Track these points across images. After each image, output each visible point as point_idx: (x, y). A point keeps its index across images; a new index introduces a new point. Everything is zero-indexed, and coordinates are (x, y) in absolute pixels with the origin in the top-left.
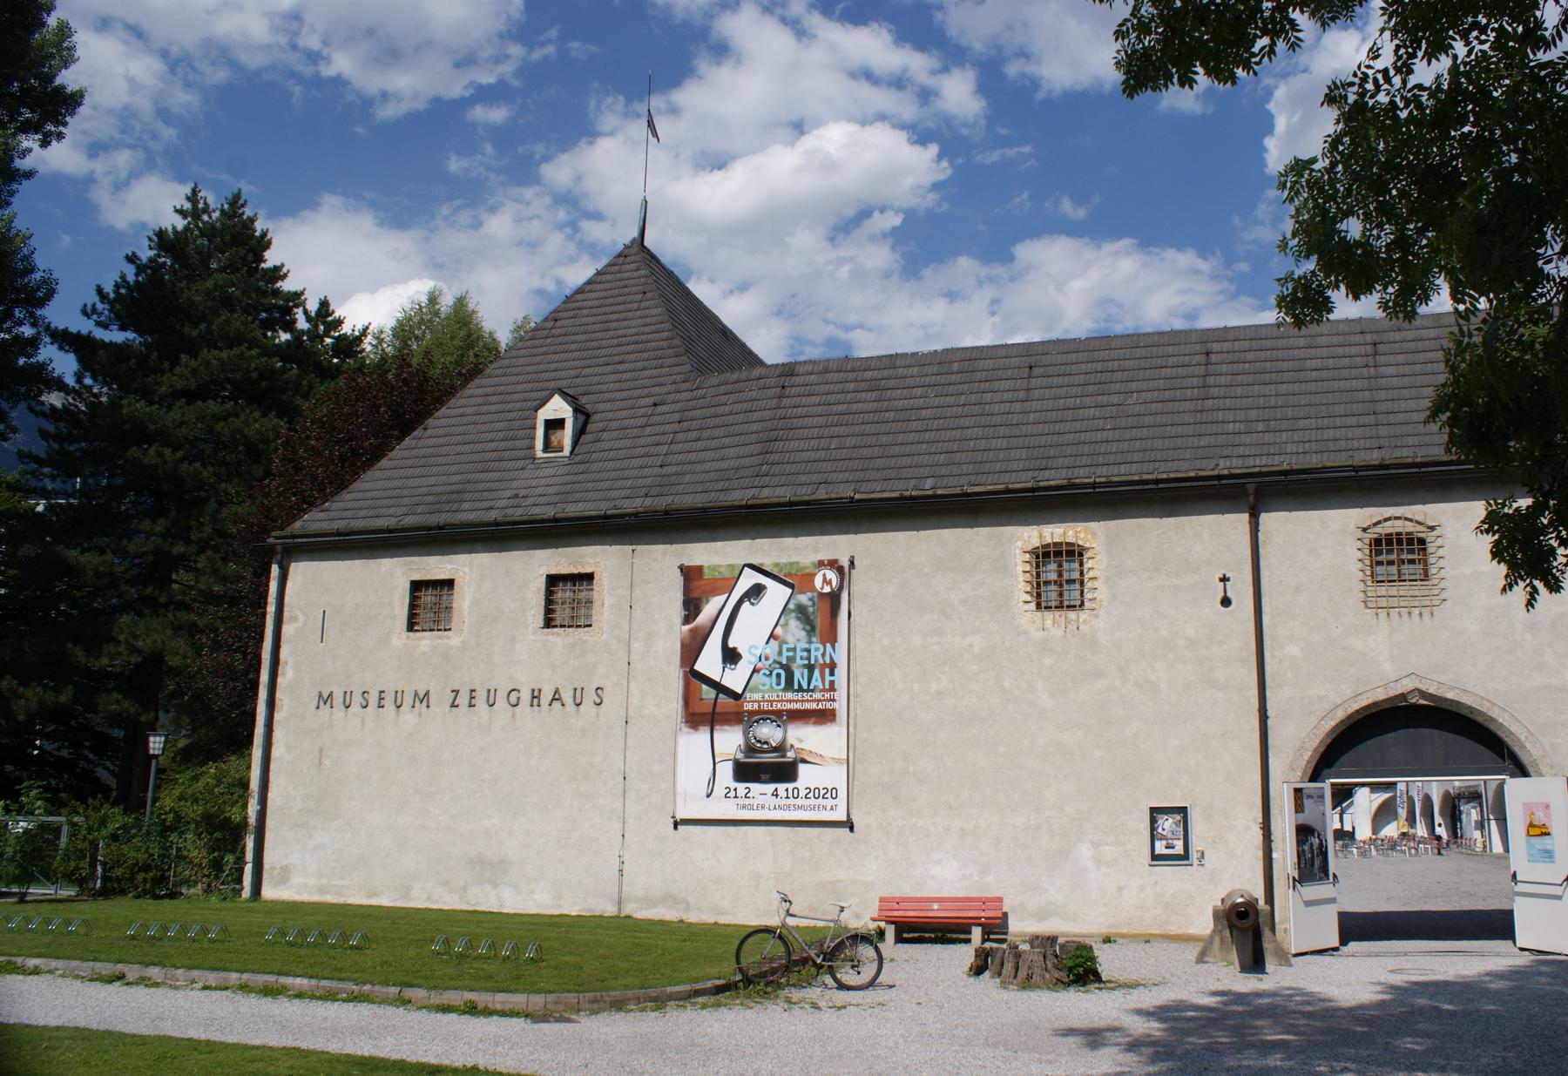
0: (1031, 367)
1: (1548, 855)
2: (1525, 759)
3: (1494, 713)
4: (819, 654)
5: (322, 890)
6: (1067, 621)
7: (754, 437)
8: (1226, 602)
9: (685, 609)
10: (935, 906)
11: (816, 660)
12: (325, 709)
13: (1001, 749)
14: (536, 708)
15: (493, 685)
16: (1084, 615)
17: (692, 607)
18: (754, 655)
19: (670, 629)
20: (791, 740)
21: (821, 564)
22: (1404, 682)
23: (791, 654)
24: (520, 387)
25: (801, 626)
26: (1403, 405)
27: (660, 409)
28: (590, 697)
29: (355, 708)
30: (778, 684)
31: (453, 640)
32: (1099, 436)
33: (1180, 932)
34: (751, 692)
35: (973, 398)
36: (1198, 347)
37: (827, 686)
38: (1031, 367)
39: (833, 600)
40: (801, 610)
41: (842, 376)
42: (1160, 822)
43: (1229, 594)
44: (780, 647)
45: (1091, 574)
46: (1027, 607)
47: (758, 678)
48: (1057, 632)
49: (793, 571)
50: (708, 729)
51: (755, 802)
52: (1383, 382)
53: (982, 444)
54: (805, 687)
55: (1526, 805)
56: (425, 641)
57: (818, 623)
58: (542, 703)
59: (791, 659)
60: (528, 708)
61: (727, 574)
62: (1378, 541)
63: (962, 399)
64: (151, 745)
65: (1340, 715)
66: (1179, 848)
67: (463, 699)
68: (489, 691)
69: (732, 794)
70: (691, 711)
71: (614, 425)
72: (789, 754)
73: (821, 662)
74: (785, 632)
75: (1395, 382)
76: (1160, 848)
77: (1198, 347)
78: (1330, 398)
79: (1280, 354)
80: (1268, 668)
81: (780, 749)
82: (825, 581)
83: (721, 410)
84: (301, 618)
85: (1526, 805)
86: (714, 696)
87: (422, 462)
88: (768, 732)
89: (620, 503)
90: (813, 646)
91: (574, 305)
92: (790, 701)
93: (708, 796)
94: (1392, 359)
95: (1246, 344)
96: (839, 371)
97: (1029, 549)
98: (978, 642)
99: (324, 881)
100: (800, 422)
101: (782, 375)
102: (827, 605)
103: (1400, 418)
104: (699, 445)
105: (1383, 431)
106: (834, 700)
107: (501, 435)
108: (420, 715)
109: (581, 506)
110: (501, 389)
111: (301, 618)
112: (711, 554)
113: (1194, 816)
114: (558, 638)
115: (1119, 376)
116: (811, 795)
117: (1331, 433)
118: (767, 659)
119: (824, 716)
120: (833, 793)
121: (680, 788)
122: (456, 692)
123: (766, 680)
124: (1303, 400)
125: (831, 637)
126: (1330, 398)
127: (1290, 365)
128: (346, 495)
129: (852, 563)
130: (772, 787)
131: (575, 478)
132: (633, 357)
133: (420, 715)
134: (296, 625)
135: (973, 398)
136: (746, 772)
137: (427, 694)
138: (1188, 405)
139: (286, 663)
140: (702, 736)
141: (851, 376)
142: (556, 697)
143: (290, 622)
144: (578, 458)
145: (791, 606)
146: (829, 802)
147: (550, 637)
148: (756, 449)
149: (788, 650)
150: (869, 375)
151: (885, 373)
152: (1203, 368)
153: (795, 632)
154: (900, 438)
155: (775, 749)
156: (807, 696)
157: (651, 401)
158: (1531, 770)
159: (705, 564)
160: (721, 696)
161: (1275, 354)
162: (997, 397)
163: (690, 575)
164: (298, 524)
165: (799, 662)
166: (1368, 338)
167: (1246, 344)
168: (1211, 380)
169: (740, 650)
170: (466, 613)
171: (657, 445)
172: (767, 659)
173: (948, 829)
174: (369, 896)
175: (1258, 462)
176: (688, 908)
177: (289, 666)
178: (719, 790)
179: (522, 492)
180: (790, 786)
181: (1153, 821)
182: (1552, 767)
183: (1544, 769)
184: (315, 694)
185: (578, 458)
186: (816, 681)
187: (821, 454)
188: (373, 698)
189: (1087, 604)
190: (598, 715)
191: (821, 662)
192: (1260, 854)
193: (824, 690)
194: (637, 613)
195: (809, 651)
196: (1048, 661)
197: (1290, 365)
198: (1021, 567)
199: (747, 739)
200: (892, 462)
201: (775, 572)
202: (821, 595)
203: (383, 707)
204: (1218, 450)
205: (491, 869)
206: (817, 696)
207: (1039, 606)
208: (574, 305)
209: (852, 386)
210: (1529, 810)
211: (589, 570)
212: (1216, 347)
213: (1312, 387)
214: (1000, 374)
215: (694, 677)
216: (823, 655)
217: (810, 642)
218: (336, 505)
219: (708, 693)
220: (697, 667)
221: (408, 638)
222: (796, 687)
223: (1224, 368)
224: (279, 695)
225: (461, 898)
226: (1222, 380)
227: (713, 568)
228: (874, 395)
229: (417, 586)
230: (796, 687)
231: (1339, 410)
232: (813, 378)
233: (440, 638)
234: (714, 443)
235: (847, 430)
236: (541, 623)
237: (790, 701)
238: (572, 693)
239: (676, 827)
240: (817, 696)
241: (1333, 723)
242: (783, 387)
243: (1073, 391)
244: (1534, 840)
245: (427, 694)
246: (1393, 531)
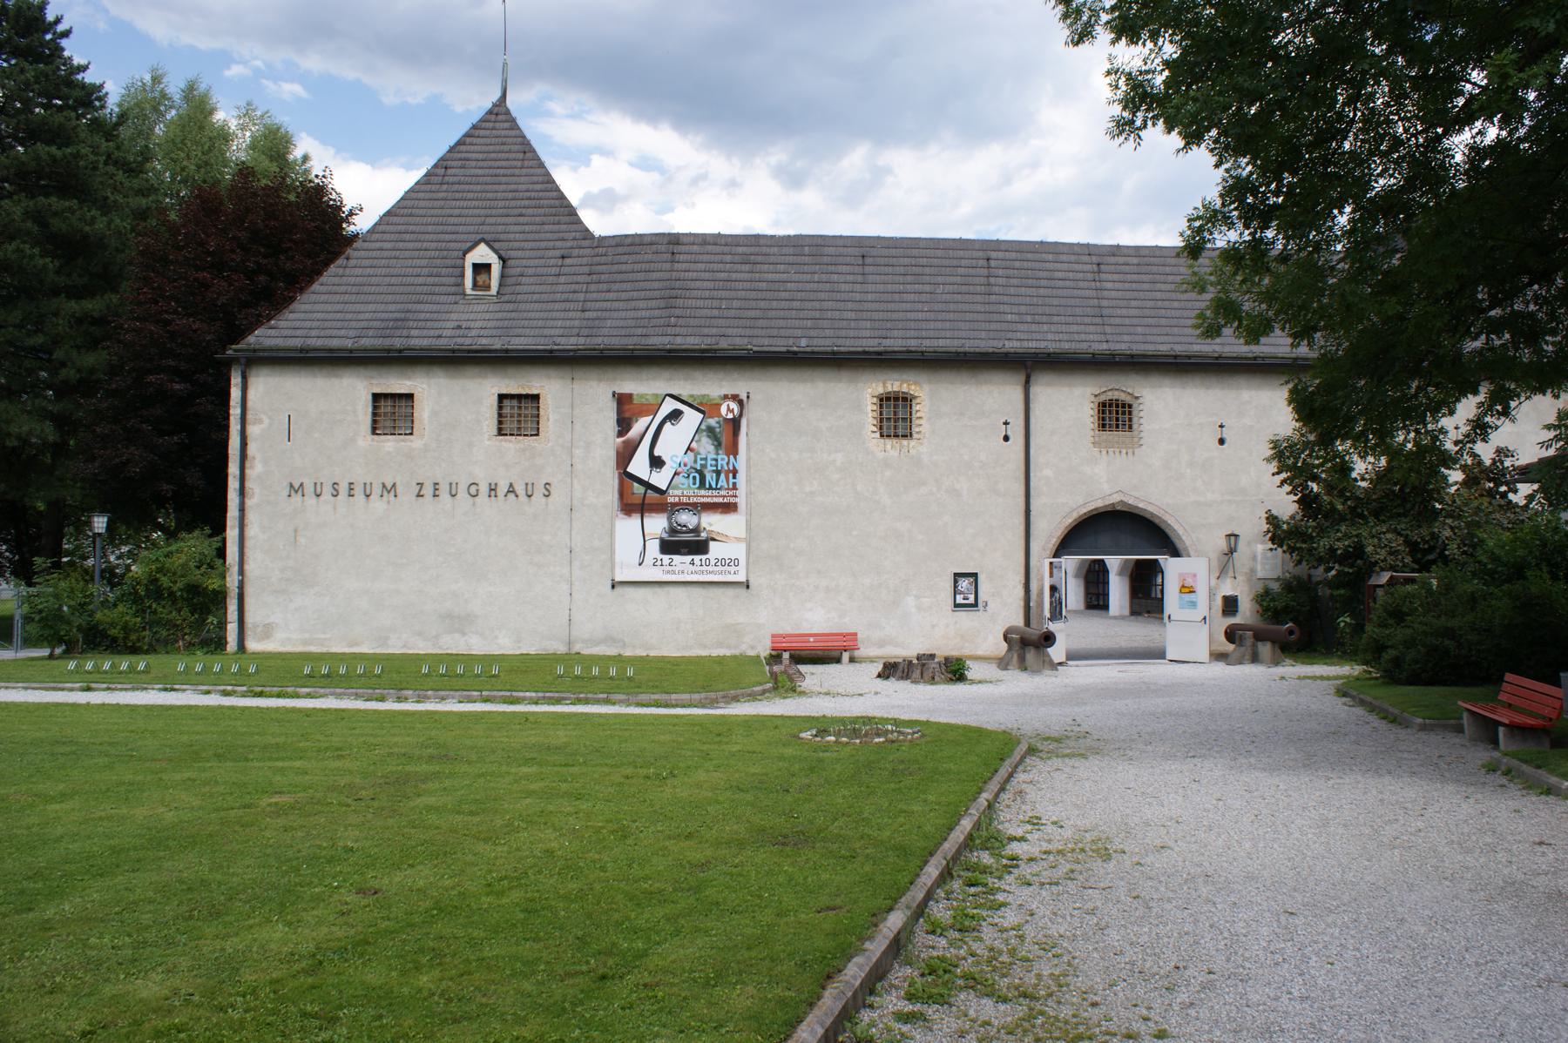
0: (863, 257)
1: (1193, 604)
2: (1179, 545)
3: (1166, 518)
4: (724, 463)
5: (306, 642)
6: (902, 446)
7: (657, 294)
8: (1006, 438)
9: (619, 426)
10: (812, 639)
11: (722, 467)
12: (297, 498)
13: (855, 533)
14: (493, 498)
15: (454, 479)
16: (913, 443)
17: (624, 424)
18: (675, 462)
19: (606, 440)
20: (704, 524)
21: (726, 397)
22: (1115, 496)
23: (703, 462)
24: (430, 228)
25: (710, 442)
26: (1119, 312)
27: (568, 261)
28: (539, 491)
29: (327, 496)
30: (694, 484)
31: (415, 443)
32: (920, 316)
33: (970, 653)
34: (673, 489)
35: (824, 277)
36: (980, 254)
37: (731, 486)
38: (863, 257)
39: (735, 424)
40: (710, 430)
41: (718, 249)
42: (960, 582)
43: (1009, 433)
44: (696, 457)
45: (919, 415)
46: (874, 435)
47: (679, 479)
48: (894, 453)
49: (704, 401)
50: (639, 515)
51: (677, 569)
52: (1105, 293)
53: (837, 314)
54: (714, 486)
55: (1180, 575)
56: (389, 444)
57: (724, 440)
58: (498, 494)
59: (704, 466)
60: (487, 499)
61: (652, 401)
62: (1104, 405)
63: (816, 277)
64: (96, 525)
65: (1075, 515)
66: (971, 600)
68: (451, 484)
69: (659, 563)
70: (625, 501)
71: (530, 271)
72: (702, 534)
73: (726, 468)
74: (699, 446)
75: (1114, 294)
76: (960, 599)
77: (980, 254)
78: (1072, 302)
79: (1037, 265)
80: (1032, 484)
81: (696, 530)
82: (728, 409)
83: (623, 267)
84: (266, 421)
85: (1180, 575)
86: (643, 491)
87: (354, 289)
88: (687, 518)
89: (558, 340)
90: (719, 457)
91: (459, 155)
92: (703, 496)
93: (640, 564)
94: (1110, 277)
95: (1013, 255)
96: (715, 244)
97: (877, 394)
98: (839, 458)
99: (307, 636)
100: (693, 285)
101: (669, 243)
102: (731, 426)
103: (1118, 321)
104: (611, 296)
105: (1108, 329)
106: (736, 496)
107: (425, 271)
108: (389, 502)
109: (522, 340)
110: (412, 228)
111: (266, 421)
112: (641, 385)
113: (981, 578)
114: (511, 445)
115: (927, 270)
116: (719, 564)
117: (1075, 328)
118: (685, 465)
119: (729, 508)
120: (736, 562)
121: (618, 558)
122: (421, 485)
123: (685, 481)
124: (1055, 302)
125: (733, 450)
126: (1072, 302)
127: (1045, 274)
128: (287, 314)
129: (748, 397)
130: (689, 558)
131: (509, 315)
132: (530, 211)
133: (389, 502)
134: (262, 426)
135: (824, 277)
136: (670, 547)
137: (394, 485)
138: (979, 298)
139: (254, 458)
140: (635, 521)
141: (726, 249)
142: (511, 490)
143: (254, 423)
144: (506, 298)
145: (703, 427)
146: (733, 569)
147: (503, 443)
148: (662, 303)
149: (701, 459)
150: (740, 250)
151: (752, 250)
152: (986, 270)
153: (706, 447)
154: (775, 304)
155: (692, 531)
156: (715, 493)
157: (558, 253)
158: (1183, 552)
159: (635, 393)
160: (649, 491)
161: (1034, 265)
162: (842, 278)
163: (622, 400)
164: (251, 339)
165: (709, 468)
166: (1094, 259)
167: (1013, 255)
168: (992, 280)
169: (664, 458)
170: (426, 422)
171: (574, 292)
172: (685, 465)
173: (817, 587)
174: (351, 646)
175: (1030, 345)
176: (624, 646)
177: (256, 462)
178: (649, 560)
179: (464, 325)
180: (704, 557)
181: (956, 582)
182: (1196, 551)
183: (1192, 553)
184: (285, 484)
185: (506, 298)
186: (722, 482)
187: (716, 313)
189: (915, 436)
190: (547, 505)
191: (726, 468)
192: (1022, 603)
193: (728, 489)
194: (578, 426)
195: (716, 460)
196: (888, 473)
197: (1045, 274)
198: (870, 407)
199: (670, 523)
200: (772, 323)
201: (690, 401)
202: (726, 420)
204: (1003, 334)
205: (460, 622)
206: (723, 493)
207: (882, 436)
208: (459, 155)
209: (728, 258)
210: (1183, 577)
211: (535, 392)
212: (993, 255)
213: (1060, 292)
214: (841, 259)
215: (626, 477)
216: (728, 464)
217: (717, 454)
218: (282, 324)
219: (638, 489)
220: (628, 470)
221: (373, 440)
222: (707, 486)
223: (1000, 272)
224: (248, 484)
225: (434, 645)
226: (1001, 281)
227: (641, 396)
228: (747, 267)
229: (377, 397)
230: (707, 486)
231: (1078, 311)
232: (695, 248)
233: (403, 441)
234: (624, 295)
235: (733, 294)
236: (495, 432)
237: (703, 496)
238: (524, 487)
239: (613, 587)
240: (723, 493)
241: (1070, 521)
242: (673, 253)
243: (897, 278)
244: (1183, 595)
245: (394, 485)
246: (1114, 398)
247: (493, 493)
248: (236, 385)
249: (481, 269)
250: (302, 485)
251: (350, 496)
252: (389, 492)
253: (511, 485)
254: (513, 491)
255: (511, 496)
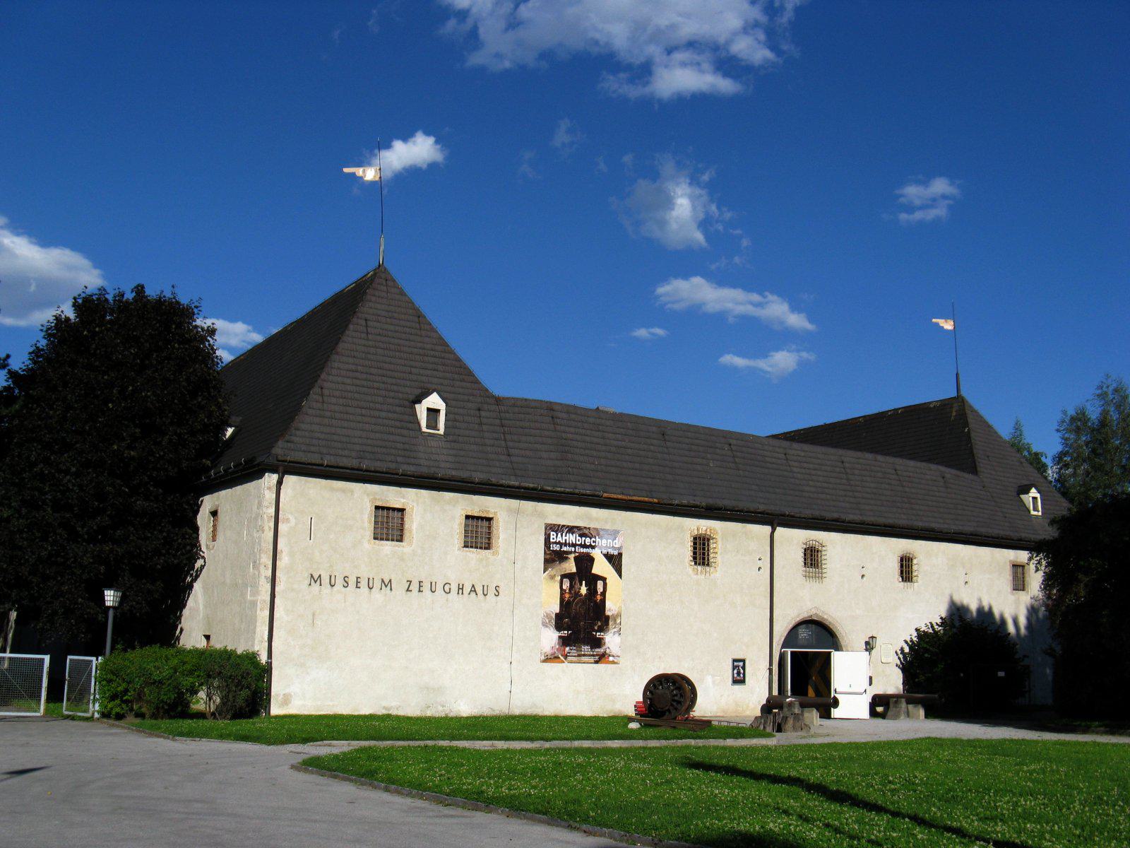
3: (837, 625)
12: (316, 587)
28: (492, 591)
29: (339, 585)
56: (388, 547)
67: (415, 586)
108: (386, 595)
133: (386, 595)
137: (390, 581)
142: (473, 590)
147: (468, 553)
170: (414, 531)
177: (284, 554)
184: (307, 575)
188: (352, 581)
203: (359, 588)
211: (491, 516)
221: (374, 543)
247: (461, 591)
248: (269, 488)
249: (433, 412)
250: (320, 576)
251: (357, 587)
252: (386, 586)
253: (473, 586)
254: (475, 591)
255: (473, 594)
